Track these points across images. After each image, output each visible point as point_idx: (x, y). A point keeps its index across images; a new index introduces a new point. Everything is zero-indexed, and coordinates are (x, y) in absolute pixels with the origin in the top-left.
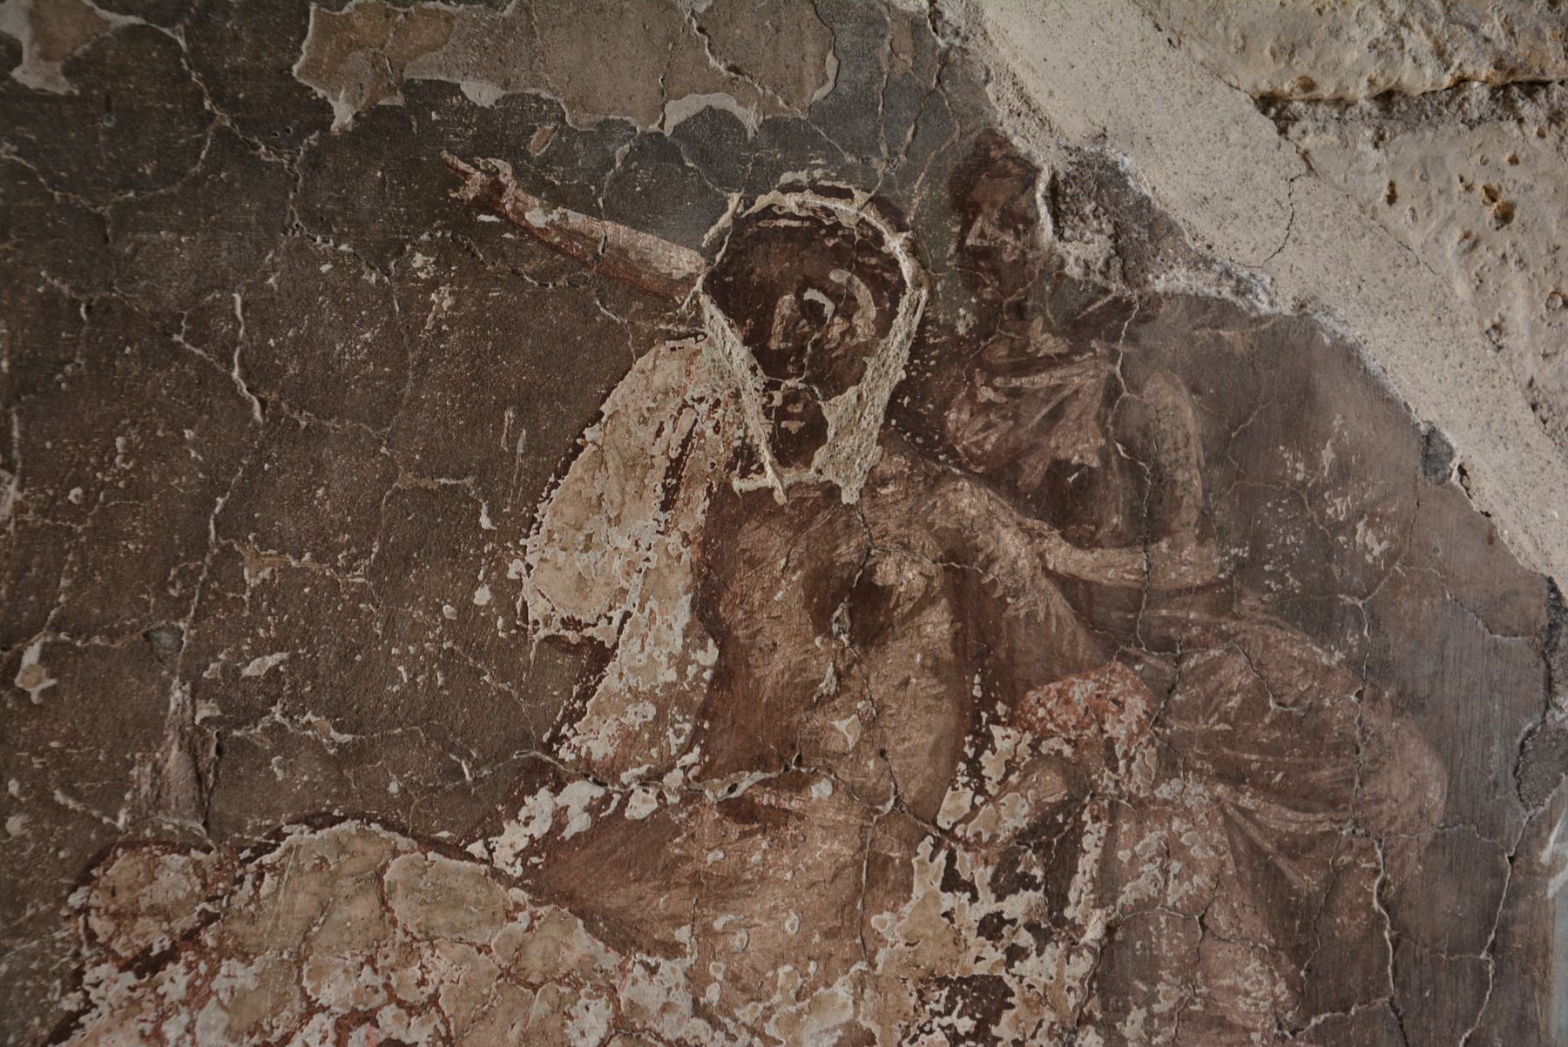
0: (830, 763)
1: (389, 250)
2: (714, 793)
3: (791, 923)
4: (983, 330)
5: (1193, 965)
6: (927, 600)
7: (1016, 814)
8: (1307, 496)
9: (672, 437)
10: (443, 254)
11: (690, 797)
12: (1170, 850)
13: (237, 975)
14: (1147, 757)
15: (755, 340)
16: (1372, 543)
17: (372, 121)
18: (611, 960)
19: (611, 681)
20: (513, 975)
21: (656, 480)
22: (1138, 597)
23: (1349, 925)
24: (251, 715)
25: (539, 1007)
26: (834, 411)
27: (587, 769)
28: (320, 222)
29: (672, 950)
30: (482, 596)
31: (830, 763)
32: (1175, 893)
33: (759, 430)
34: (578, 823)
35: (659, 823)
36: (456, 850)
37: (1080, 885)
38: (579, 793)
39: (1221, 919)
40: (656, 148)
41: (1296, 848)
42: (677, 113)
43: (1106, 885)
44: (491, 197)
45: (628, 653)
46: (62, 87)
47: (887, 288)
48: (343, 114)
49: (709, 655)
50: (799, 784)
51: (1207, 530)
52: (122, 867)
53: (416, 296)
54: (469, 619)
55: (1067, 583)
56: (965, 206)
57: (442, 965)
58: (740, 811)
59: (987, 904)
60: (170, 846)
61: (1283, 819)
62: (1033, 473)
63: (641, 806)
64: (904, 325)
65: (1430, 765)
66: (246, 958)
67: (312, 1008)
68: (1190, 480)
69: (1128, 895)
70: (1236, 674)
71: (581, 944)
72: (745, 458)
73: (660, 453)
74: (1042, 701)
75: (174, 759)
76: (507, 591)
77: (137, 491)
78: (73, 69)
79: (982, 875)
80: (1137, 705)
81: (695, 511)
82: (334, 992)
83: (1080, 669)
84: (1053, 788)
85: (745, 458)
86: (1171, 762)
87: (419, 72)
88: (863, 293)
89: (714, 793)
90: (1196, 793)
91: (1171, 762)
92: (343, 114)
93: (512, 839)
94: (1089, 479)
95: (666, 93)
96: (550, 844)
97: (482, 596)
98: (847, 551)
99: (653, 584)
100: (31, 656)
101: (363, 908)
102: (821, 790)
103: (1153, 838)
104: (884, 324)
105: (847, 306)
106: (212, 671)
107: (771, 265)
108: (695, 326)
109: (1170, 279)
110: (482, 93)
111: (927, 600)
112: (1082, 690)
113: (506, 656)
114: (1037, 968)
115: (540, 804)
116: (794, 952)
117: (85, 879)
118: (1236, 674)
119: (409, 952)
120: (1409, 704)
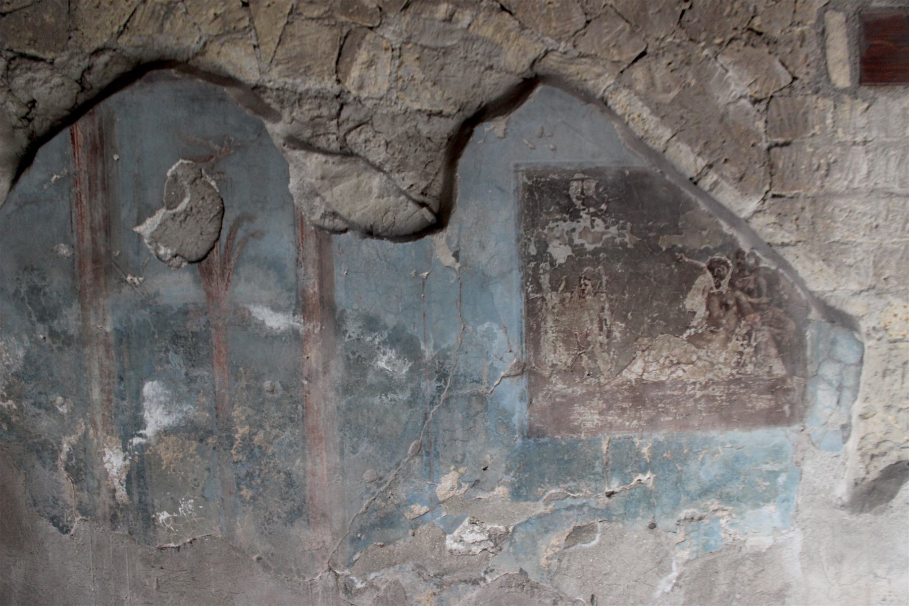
0: (722, 325)
1: (669, 265)
2: (709, 329)
3: (718, 345)
4: (740, 271)
5: (766, 349)
6: (734, 305)
7: (744, 331)
8: (778, 291)
9: (703, 287)
10: (676, 265)
11: (706, 329)
12: (763, 335)
13: (653, 352)
14: (760, 324)
15: (713, 274)
16: (786, 297)
17: (667, 249)
18: (697, 350)
19: (696, 316)
20: (685, 352)
21: (701, 292)
22: (759, 304)
23: (784, 343)
24: (654, 321)
25: (688, 356)
26: (722, 282)
27: (693, 327)
28: (661, 262)
29: (704, 349)
30: (681, 306)
31: (722, 325)
32: (764, 340)
33: (713, 285)
34: (693, 334)
35: (702, 334)
36: (678, 337)
37: (752, 340)
38: (693, 330)
39: (769, 343)
40: (700, 251)
41: (778, 334)
42: (703, 247)
43: (755, 340)
44: (681, 258)
45: (698, 313)
46: (633, 247)
47: (728, 267)
48: (664, 249)
49: (708, 313)
50: (718, 328)
51: (767, 296)
52: (640, 340)
53: (672, 270)
54: (679, 310)
55: (750, 303)
56: (737, 257)
57: (677, 351)
58: (712, 332)
59: (741, 343)
60: (645, 337)
61: (777, 331)
62: (746, 289)
63: (700, 331)
64: (730, 272)
65: (793, 323)
66: (654, 350)
67: (662, 356)
68: (765, 290)
69: (759, 340)
70: (770, 314)
71: (693, 348)
72: (712, 288)
73: (702, 287)
74: (748, 317)
75: (646, 326)
76: (684, 306)
77: (641, 295)
78: (634, 245)
79: (741, 339)
80: (759, 318)
81: (706, 295)
82: (664, 354)
83: (752, 313)
84: (749, 328)
85: (712, 288)
86: (763, 324)
87: (674, 243)
88: (725, 268)
89: (709, 329)
90: (766, 328)
91: (763, 324)
92: (664, 249)
93: (685, 336)
94: (753, 290)
95: (702, 245)
96: (689, 336)
97: (681, 306)
98: (724, 300)
99: (701, 305)
100: (629, 314)
101: (667, 344)
102: (721, 329)
103: (761, 334)
104: (728, 272)
105: (723, 270)
106: (650, 316)
107: (714, 265)
108: (705, 273)
109: (762, 265)
110: (680, 246)
111: (734, 305)
112: (752, 316)
113: (684, 313)
114: (748, 350)
115: (688, 331)
116: (718, 349)
117: (636, 341)
118: (770, 314)
119: (673, 350)
120: (791, 316)
